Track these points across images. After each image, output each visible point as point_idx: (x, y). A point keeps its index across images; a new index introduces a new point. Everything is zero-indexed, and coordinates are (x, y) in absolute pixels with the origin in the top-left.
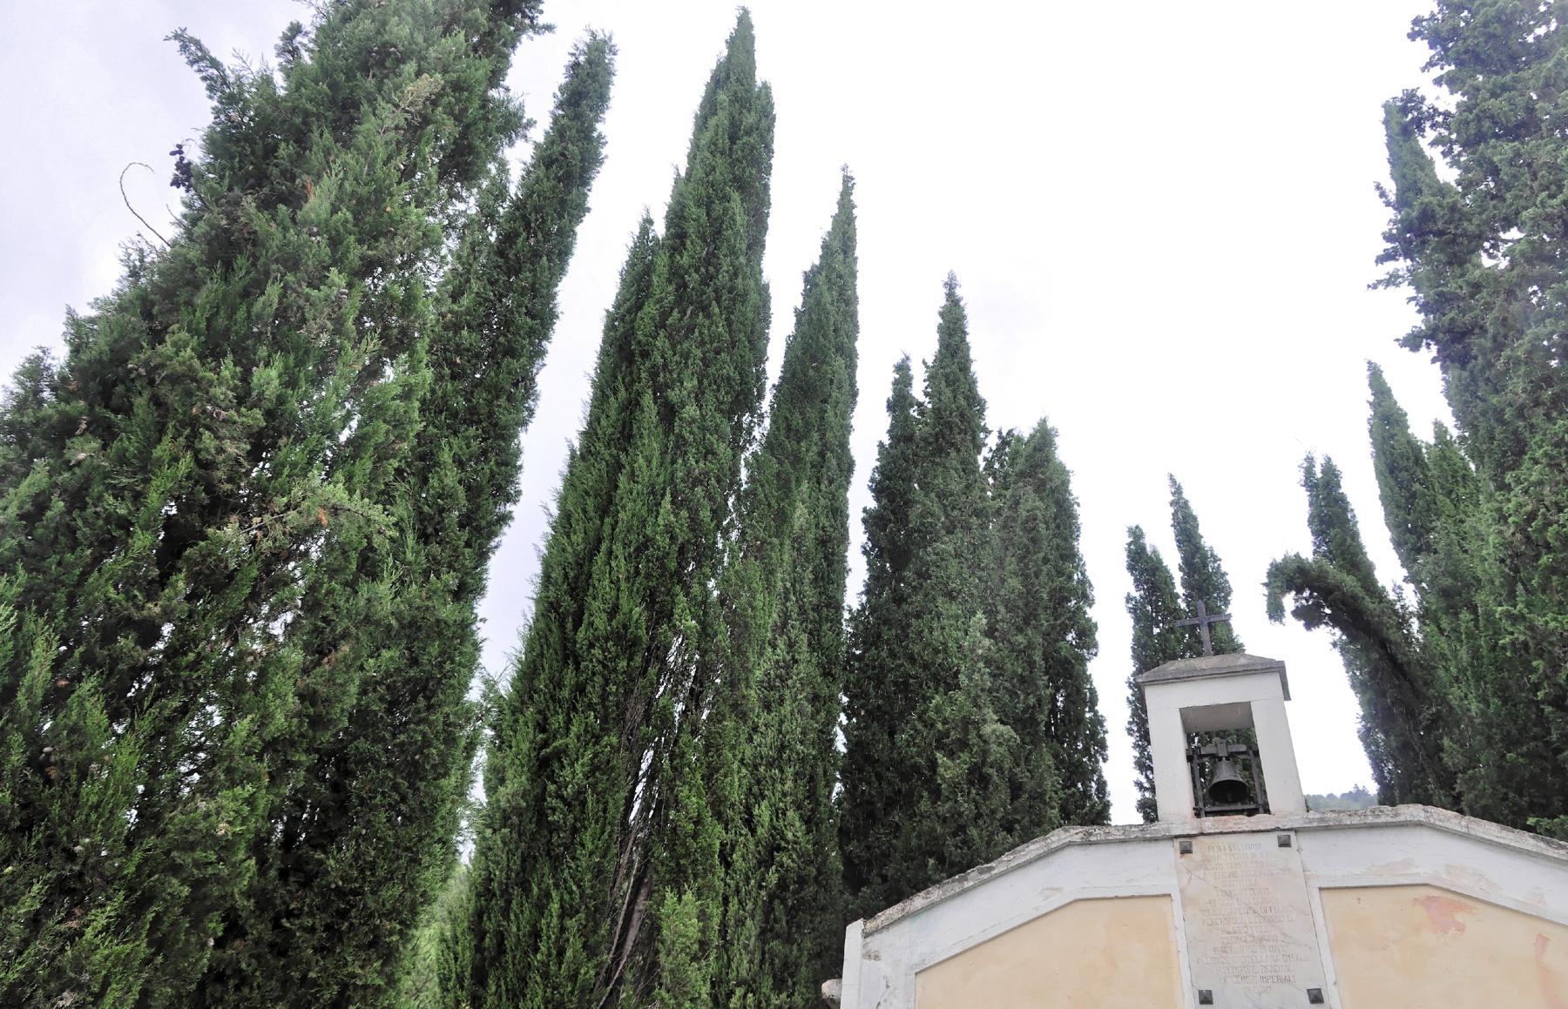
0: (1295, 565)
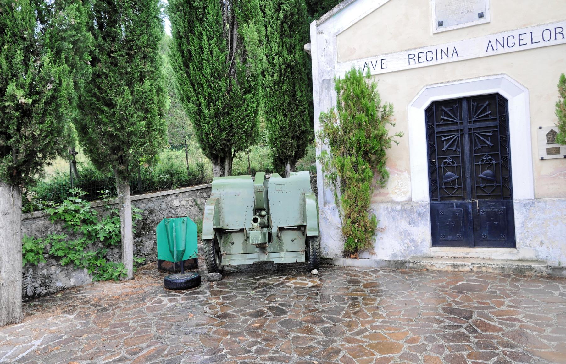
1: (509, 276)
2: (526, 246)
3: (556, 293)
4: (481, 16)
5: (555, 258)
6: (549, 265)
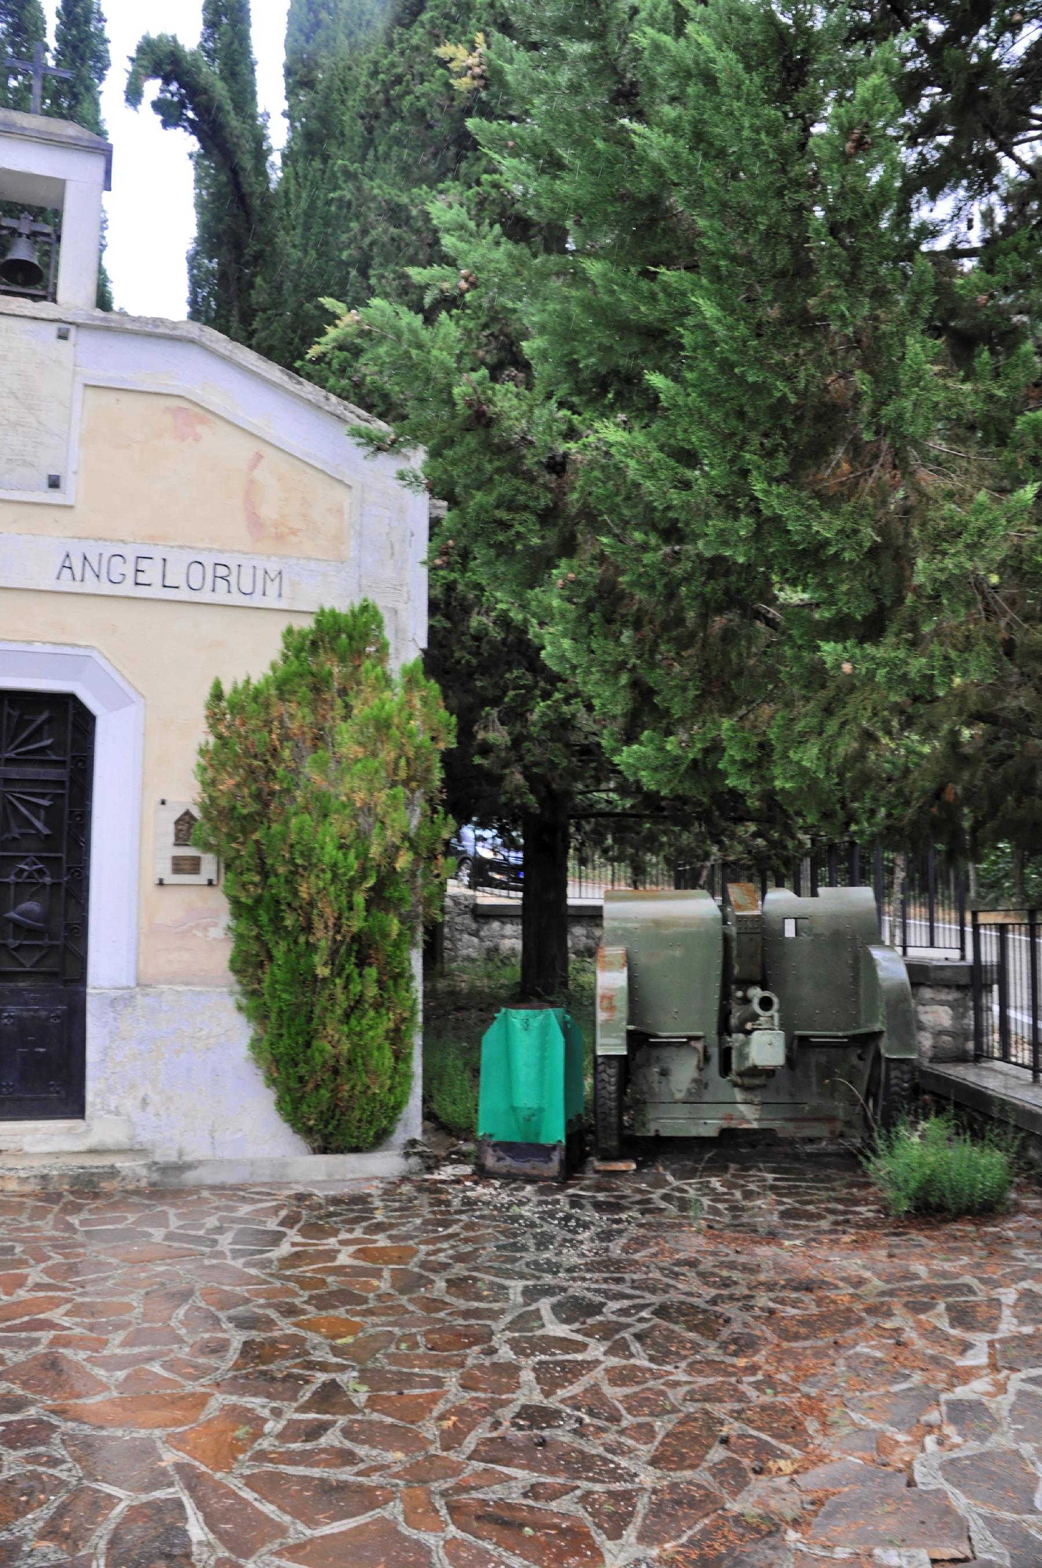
0: (168, 49)
1: (60, 1196)
2: (109, 1112)
3: (158, 1234)
4: (54, 483)
5: (171, 1140)
6: (157, 1159)
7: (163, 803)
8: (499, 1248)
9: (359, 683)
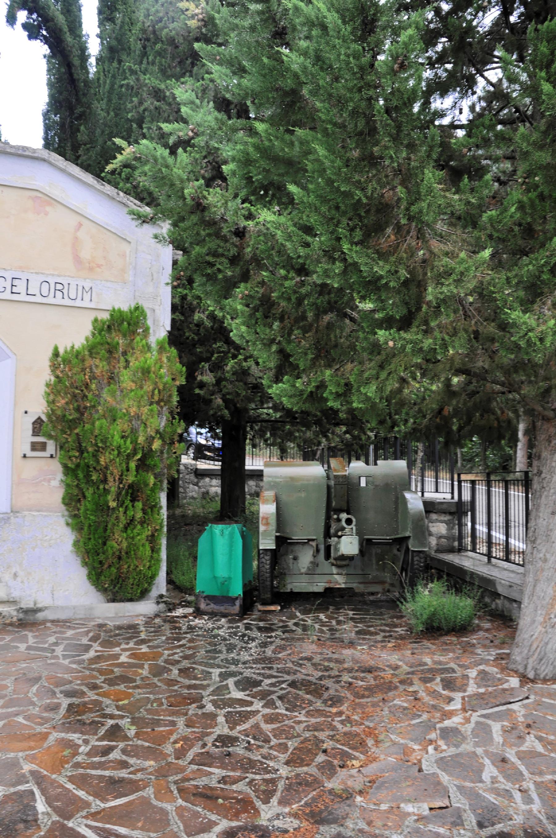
3: (22, 647)
5: (30, 596)
6: (22, 606)
7: (26, 412)
8: (207, 652)
9: (133, 349)
